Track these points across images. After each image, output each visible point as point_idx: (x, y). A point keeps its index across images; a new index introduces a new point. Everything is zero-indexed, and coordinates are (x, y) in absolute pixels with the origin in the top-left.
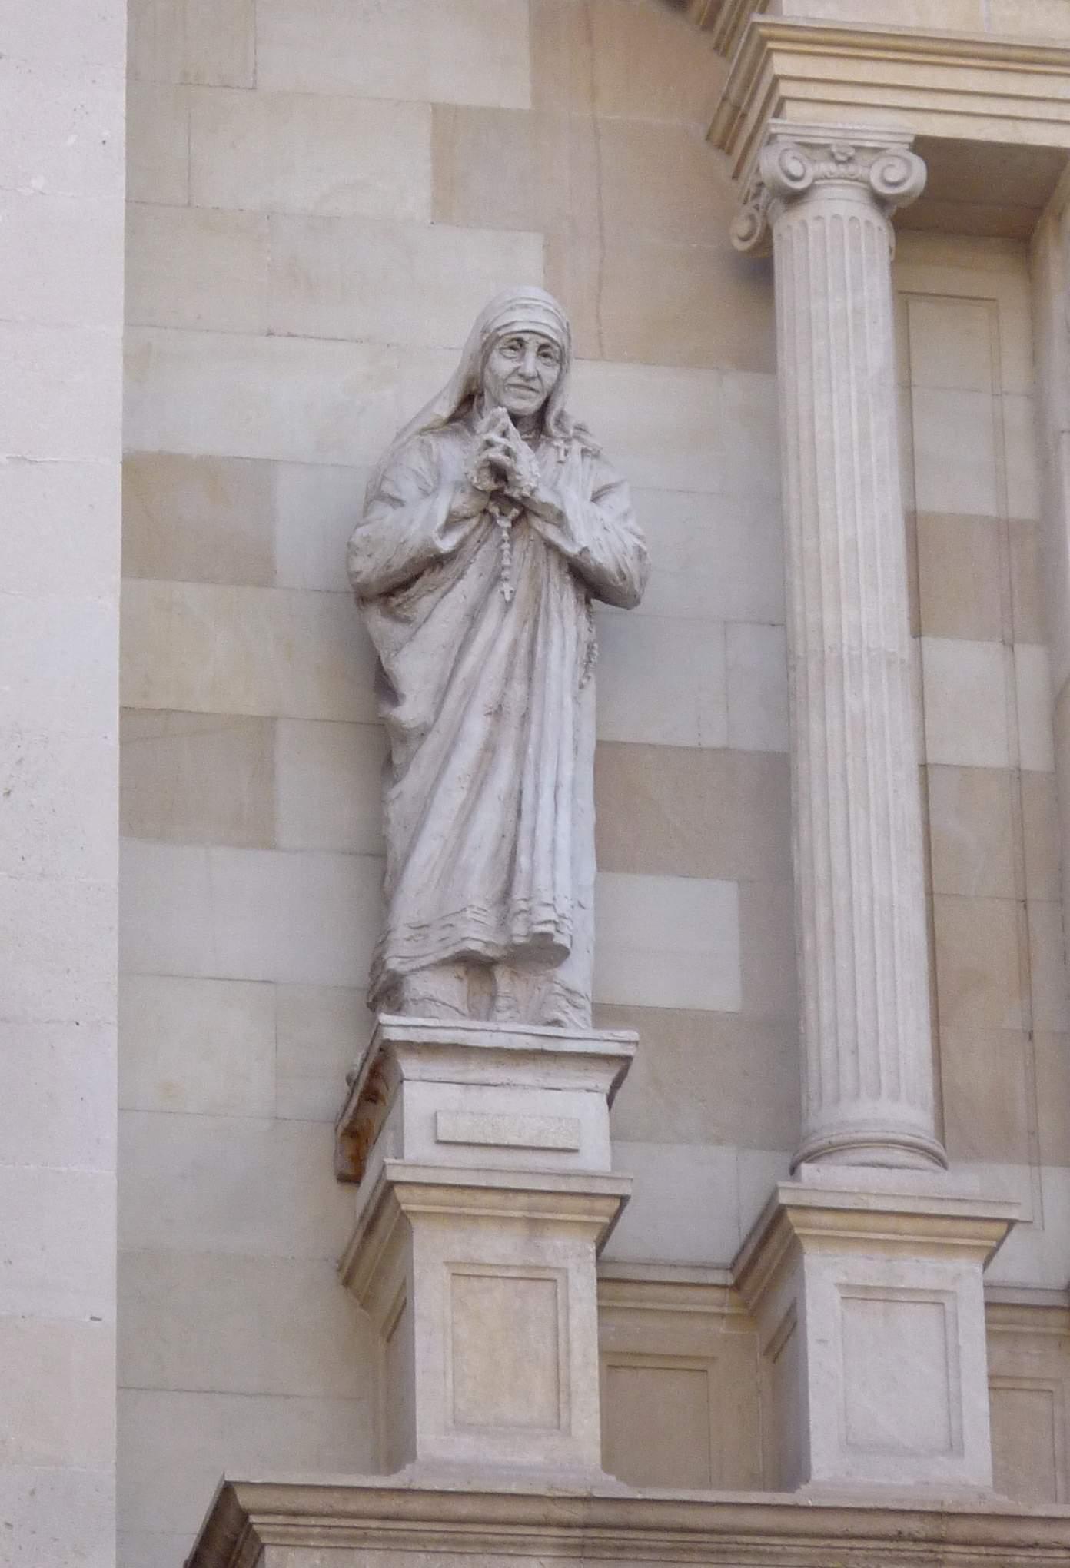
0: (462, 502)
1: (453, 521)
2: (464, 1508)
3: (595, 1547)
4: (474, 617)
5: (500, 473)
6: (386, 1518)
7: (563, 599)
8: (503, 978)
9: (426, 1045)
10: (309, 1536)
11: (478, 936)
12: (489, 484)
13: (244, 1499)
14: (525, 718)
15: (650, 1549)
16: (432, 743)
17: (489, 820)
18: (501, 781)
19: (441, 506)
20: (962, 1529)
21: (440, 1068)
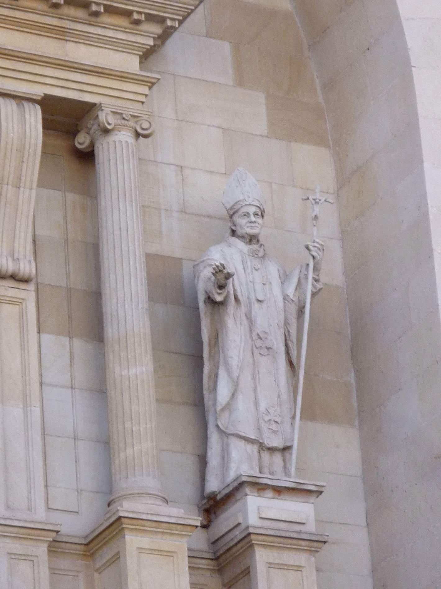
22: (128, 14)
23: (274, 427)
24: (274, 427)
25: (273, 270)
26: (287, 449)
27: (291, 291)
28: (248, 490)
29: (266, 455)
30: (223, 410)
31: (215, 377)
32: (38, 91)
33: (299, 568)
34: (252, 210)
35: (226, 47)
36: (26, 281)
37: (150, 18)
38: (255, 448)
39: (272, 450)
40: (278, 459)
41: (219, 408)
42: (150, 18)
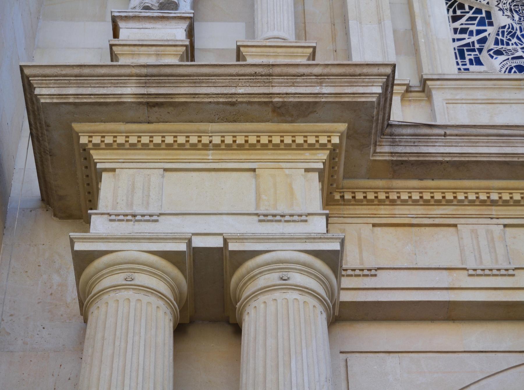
3: (149, 83)
6: (76, 76)
9: (126, 17)
10: (50, 84)
13: (27, 71)
15: (169, 83)
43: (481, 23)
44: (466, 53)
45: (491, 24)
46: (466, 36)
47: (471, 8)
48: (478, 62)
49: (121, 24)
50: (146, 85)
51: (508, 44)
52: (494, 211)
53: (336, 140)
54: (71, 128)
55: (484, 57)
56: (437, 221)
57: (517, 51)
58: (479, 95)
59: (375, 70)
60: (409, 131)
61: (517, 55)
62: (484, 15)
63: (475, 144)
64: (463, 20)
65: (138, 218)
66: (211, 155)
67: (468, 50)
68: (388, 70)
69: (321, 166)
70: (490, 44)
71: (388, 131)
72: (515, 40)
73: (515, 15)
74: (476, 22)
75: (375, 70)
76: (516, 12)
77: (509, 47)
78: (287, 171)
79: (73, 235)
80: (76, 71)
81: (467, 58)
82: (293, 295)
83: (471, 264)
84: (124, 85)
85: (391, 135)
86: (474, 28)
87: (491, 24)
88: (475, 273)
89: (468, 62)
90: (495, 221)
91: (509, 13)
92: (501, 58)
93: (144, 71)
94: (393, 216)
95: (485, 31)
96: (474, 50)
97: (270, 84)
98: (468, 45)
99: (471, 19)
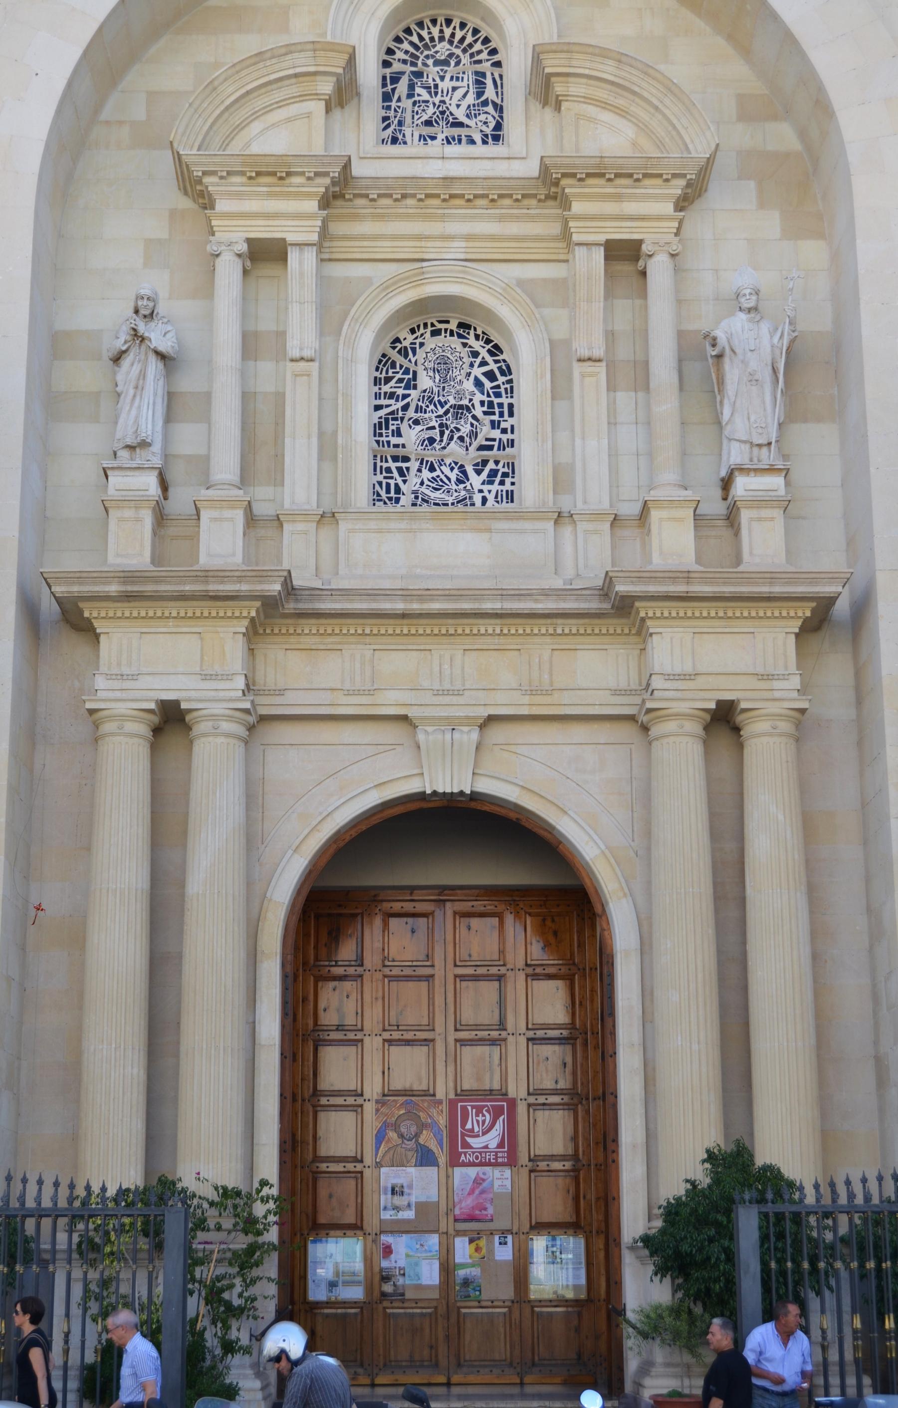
0: (129, 338)
1: (126, 342)
2: (95, 575)
4: (132, 365)
5: (134, 330)
7: (152, 358)
8: (138, 450)
11: (129, 441)
12: (133, 333)
14: (143, 388)
16: (123, 395)
17: (134, 412)
18: (136, 404)
19: (122, 340)
20: (211, 574)
21: (116, 473)
22: (660, 176)
23: (760, 430)
24: (760, 430)
25: (765, 327)
26: (770, 444)
27: (776, 340)
28: (736, 473)
29: (756, 450)
30: (726, 424)
31: (721, 402)
32: (602, 238)
33: (772, 519)
34: (747, 291)
35: (752, 184)
36: (600, 361)
37: (675, 176)
38: (748, 446)
39: (760, 446)
40: (765, 450)
41: (724, 424)
42: (675, 176)
43: (407, 387)
44: (391, 422)
45: (415, 387)
46: (392, 402)
47: (401, 367)
48: (399, 435)
49: (109, 473)
50: (125, 583)
51: (425, 412)
52: (368, 640)
53: (253, 614)
54: (78, 607)
55: (404, 428)
56: (329, 647)
57: (431, 419)
58: (372, 525)
59: (276, 574)
60: (307, 592)
61: (431, 424)
62: (411, 376)
63: (352, 601)
64: (392, 383)
65: (125, 677)
66: (171, 623)
67: (393, 419)
68: (285, 574)
69: (244, 630)
70: (411, 413)
71: (293, 592)
72: (432, 407)
73: (437, 376)
74: (403, 385)
75: (276, 574)
76: (438, 371)
77: (426, 416)
78: (222, 635)
79: (84, 698)
80: (78, 575)
81: (391, 427)
82: (221, 740)
83: (347, 686)
84: (109, 583)
85: (295, 595)
86: (400, 392)
87: (415, 387)
88: (349, 693)
89: (390, 431)
90: (368, 646)
91: (431, 373)
92: (418, 428)
93: (122, 574)
94: (299, 643)
95: (409, 395)
96: (396, 419)
97: (207, 582)
98: (392, 413)
99: (400, 381)
